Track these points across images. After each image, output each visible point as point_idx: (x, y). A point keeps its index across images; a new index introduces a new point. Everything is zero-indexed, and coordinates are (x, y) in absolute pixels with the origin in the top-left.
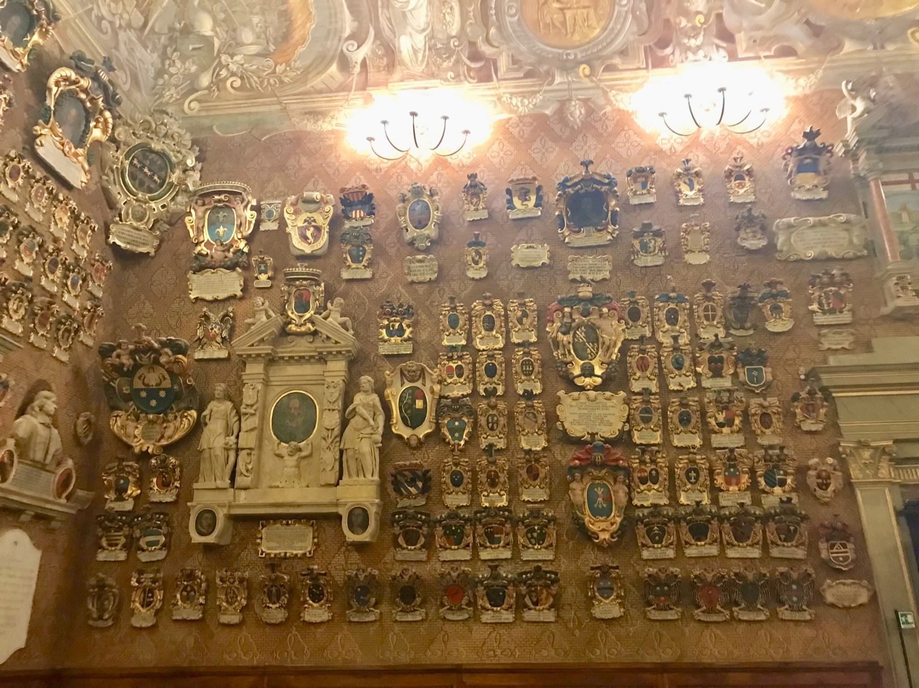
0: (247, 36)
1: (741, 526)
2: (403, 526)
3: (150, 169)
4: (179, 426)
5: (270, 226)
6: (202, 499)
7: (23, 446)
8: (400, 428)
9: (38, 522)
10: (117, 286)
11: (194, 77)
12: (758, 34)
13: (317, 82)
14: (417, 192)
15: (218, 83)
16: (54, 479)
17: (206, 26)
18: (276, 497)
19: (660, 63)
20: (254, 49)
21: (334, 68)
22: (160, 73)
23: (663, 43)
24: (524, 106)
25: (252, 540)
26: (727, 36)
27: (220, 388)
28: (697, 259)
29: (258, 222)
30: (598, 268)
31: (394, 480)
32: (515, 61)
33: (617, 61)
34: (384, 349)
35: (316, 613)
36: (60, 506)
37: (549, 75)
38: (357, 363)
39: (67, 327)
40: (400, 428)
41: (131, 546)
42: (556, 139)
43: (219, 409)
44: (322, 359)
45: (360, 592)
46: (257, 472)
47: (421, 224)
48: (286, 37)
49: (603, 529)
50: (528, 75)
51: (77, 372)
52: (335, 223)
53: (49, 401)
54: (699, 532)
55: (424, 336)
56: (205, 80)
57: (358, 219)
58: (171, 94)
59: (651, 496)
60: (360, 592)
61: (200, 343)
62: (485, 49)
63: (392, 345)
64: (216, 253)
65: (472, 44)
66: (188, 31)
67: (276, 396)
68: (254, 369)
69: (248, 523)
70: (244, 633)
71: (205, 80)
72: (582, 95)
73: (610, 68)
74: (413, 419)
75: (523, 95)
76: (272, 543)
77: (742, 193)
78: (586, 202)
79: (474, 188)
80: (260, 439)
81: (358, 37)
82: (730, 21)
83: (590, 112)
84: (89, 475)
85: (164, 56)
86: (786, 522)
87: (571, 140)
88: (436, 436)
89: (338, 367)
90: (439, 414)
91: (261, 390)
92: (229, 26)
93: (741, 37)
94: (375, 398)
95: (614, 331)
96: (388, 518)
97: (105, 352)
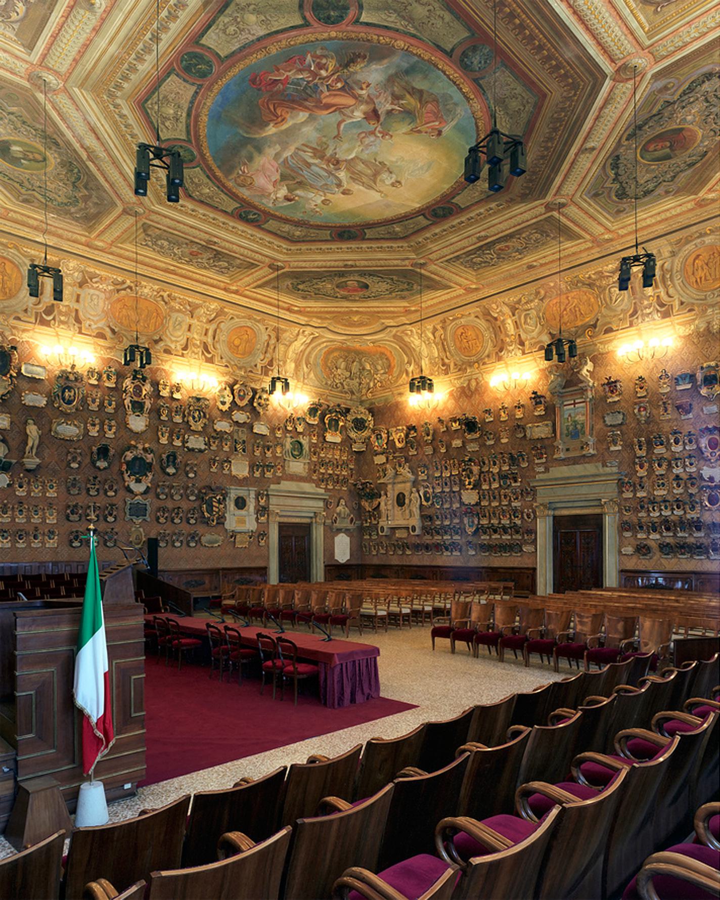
0: (379, 368)
1: (505, 530)
2: (426, 530)
3: (360, 424)
4: (375, 503)
5: (391, 438)
6: (381, 524)
7: (339, 514)
8: (424, 503)
9: (347, 531)
10: (357, 462)
11: (368, 384)
12: (533, 341)
13: (400, 382)
14: (426, 424)
15: (375, 385)
16: (349, 521)
17: (368, 367)
18: (397, 523)
19: (500, 359)
20: (382, 372)
21: (404, 375)
22: (360, 384)
23: (501, 350)
24: (458, 383)
25: (394, 533)
26: (522, 344)
27: (382, 492)
28: (504, 441)
29: (388, 437)
30: (473, 447)
31: (423, 517)
32: (455, 365)
33: (486, 359)
34: (420, 478)
35: (408, 552)
36: (351, 526)
37: (466, 369)
38: (415, 483)
39: (345, 481)
40: (424, 503)
41: (370, 535)
42: (467, 396)
43: (383, 498)
44: (404, 482)
45: (417, 547)
46: (394, 516)
47: (428, 435)
48: (390, 366)
49: (470, 530)
50: (459, 370)
51: (350, 491)
52: (407, 436)
53: (342, 502)
54: (495, 531)
55: (431, 472)
56: (372, 385)
57: (413, 434)
58: (364, 391)
59: (484, 522)
60: (417, 547)
61: (379, 478)
62: (446, 361)
63: (422, 477)
64: (379, 450)
65: (442, 359)
66: (364, 369)
67: (396, 493)
68: (390, 486)
69: (393, 529)
70: (395, 557)
71: (372, 385)
72: (475, 377)
73: (484, 364)
74: (427, 500)
75: (458, 379)
76: (399, 534)
77: (519, 414)
78: (470, 425)
79: (440, 421)
80: (393, 507)
81: (409, 363)
82: (523, 336)
83: (478, 383)
84: (359, 517)
85: (360, 378)
86: (516, 529)
87: (471, 397)
88: (433, 504)
89: (409, 485)
90: (433, 498)
91: (392, 493)
92: (373, 365)
93: (527, 343)
94: (417, 495)
95: (476, 469)
96: (423, 528)
97: (355, 485)
